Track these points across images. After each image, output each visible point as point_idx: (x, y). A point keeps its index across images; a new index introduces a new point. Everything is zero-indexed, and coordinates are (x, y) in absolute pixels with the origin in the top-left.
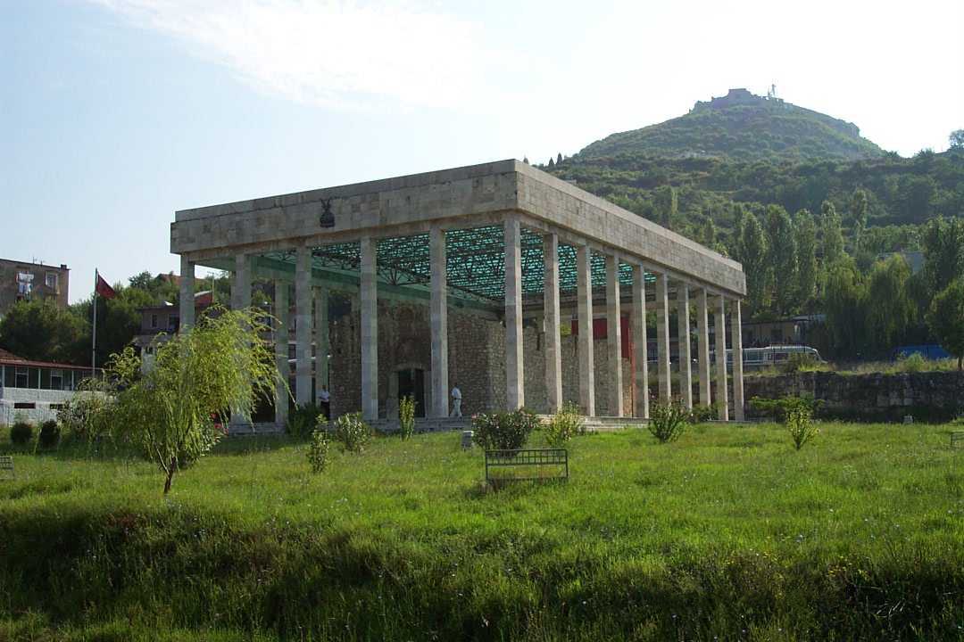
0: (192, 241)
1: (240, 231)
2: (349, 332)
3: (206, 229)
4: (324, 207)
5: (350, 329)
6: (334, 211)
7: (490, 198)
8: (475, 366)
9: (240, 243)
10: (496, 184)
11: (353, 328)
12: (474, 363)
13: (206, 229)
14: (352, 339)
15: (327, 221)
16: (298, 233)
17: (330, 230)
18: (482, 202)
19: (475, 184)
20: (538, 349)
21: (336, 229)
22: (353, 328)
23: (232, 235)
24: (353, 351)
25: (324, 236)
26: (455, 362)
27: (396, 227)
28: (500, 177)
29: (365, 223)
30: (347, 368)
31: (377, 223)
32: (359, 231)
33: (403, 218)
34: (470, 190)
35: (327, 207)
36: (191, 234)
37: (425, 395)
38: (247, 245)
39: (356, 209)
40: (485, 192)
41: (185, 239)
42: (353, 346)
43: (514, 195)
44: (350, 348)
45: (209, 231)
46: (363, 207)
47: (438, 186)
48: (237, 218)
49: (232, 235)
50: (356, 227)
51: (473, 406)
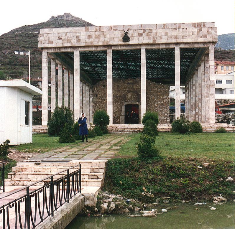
1: (79, 40)
4: (125, 33)
7: (205, 36)
8: (162, 104)
12: (163, 103)
15: (126, 38)
16: (111, 43)
17: (127, 43)
18: (201, 37)
21: (131, 42)
27: (159, 44)
29: (146, 41)
33: (164, 41)
35: (126, 34)
41: (47, 42)
45: (61, 39)
51: (161, 120)
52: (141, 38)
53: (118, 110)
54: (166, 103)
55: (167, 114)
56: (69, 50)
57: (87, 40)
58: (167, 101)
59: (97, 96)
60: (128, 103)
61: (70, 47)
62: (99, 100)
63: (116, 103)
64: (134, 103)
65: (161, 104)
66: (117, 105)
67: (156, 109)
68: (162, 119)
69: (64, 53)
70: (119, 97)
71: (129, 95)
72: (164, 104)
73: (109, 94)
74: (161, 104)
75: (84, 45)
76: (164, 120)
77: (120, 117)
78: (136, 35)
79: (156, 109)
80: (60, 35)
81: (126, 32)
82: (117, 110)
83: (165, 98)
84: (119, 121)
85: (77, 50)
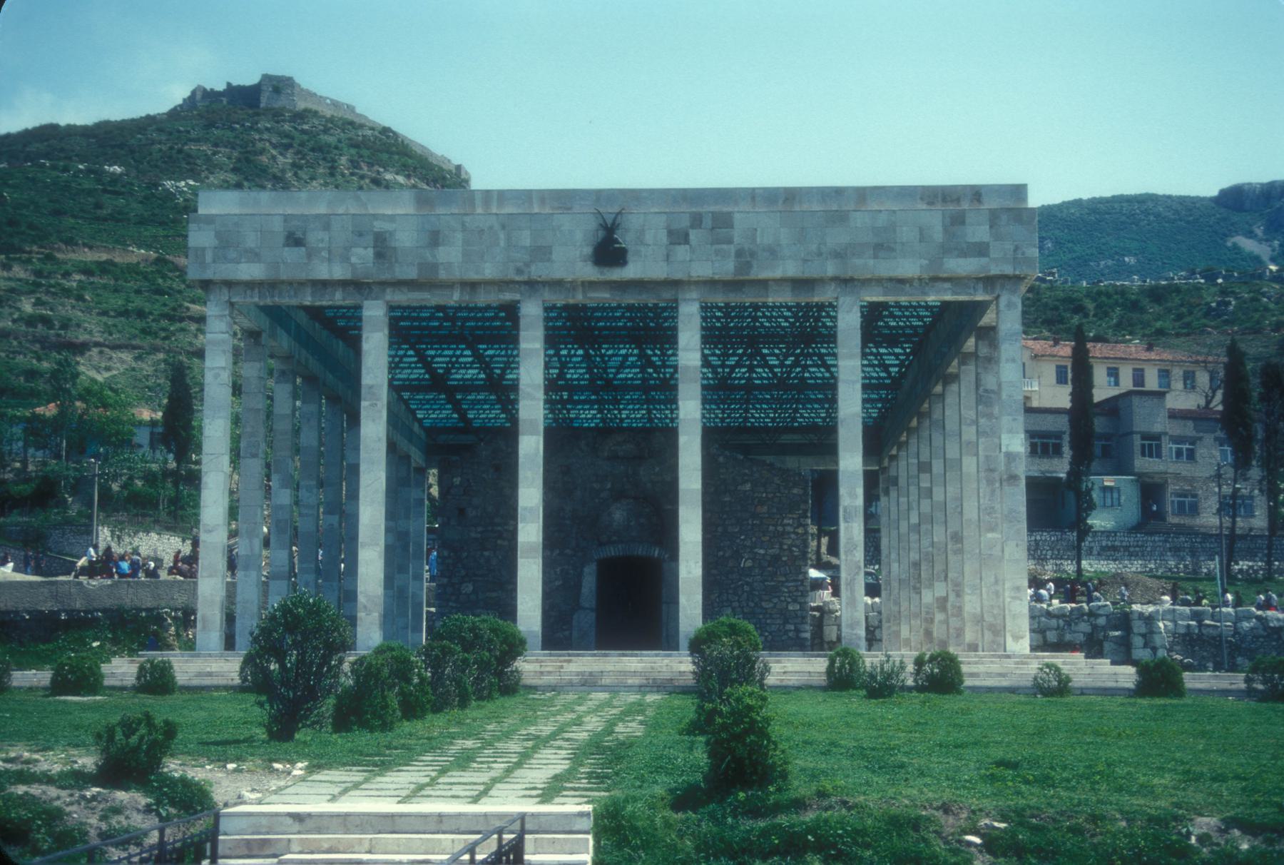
7: (981, 250)
8: (776, 558)
9: (386, 276)
21: (631, 271)
23: (363, 256)
25: (591, 285)
27: (764, 284)
29: (702, 270)
31: (726, 268)
32: (675, 284)
33: (790, 269)
38: (399, 284)
39: (678, 237)
49: (363, 256)
50: (678, 276)
51: (770, 633)
52: (681, 252)
54: (791, 551)
55: (798, 607)
56: (338, 298)
59: (462, 512)
60: (612, 551)
61: (344, 284)
62: (473, 535)
64: (640, 551)
65: (768, 558)
67: (747, 583)
68: (774, 628)
69: (315, 313)
71: (618, 514)
72: (784, 559)
73: (525, 509)
74: (768, 558)
75: (411, 273)
76: (786, 632)
77: (575, 617)
79: (747, 583)
83: (789, 529)
84: (567, 633)
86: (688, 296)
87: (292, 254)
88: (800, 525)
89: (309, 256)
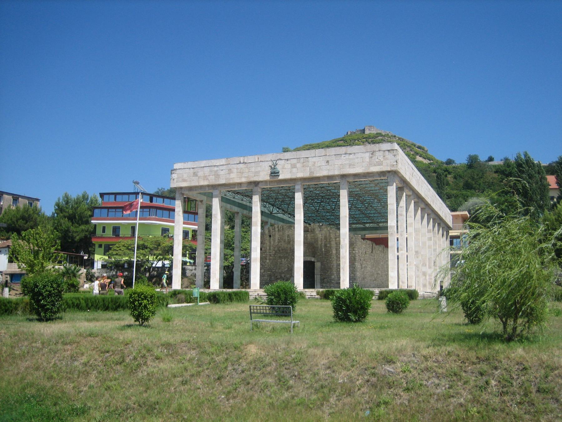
0: (184, 180)
1: (217, 176)
2: (268, 238)
3: (195, 174)
5: (268, 237)
6: (279, 168)
7: (380, 164)
10: (384, 156)
11: (270, 236)
13: (195, 174)
14: (270, 242)
18: (375, 165)
19: (371, 156)
20: (372, 252)
21: (281, 177)
22: (270, 236)
24: (270, 249)
26: (335, 258)
28: (387, 152)
30: (266, 259)
34: (367, 160)
36: (185, 176)
37: (315, 276)
39: (293, 166)
40: (377, 160)
41: (181, 180)
42: (270, 247)
43: (396, 163)
44: (268, 248)
45: (197, 176)
46: (298, 165)
47: (347, 156)
48: (216, 169)
52: (294, 170)
53: (288, 268)
57: (228, 176)
58: (353, 255)
63: (286, 260)
66: (287, 262)
70: (289, 251)
78: (288, 166)
80: (196, 170)
81: (275, 163)
82: (286, 269)
85: (216, 189)
86: (298, 183)
87: (195, 178)
88: (354, 250)
89: (199, 178)
